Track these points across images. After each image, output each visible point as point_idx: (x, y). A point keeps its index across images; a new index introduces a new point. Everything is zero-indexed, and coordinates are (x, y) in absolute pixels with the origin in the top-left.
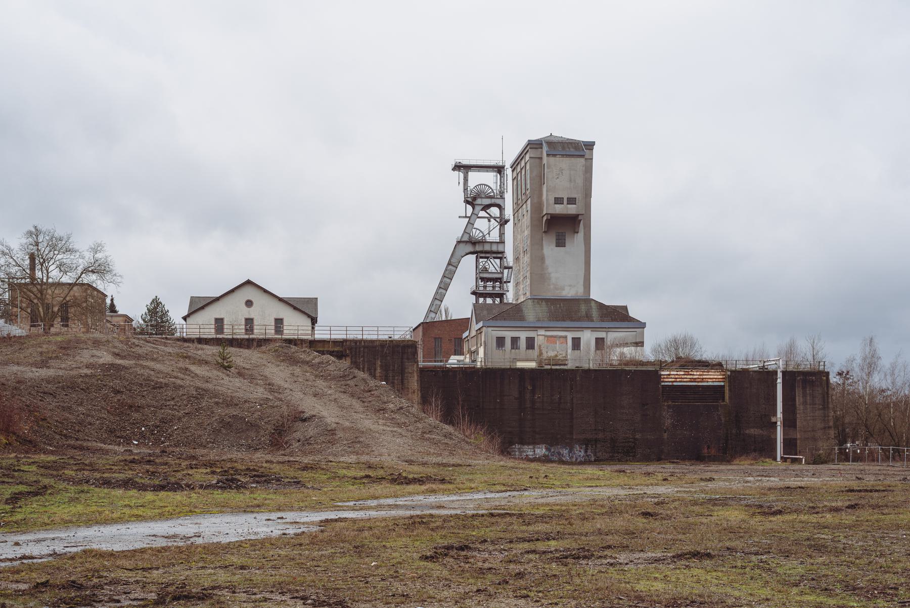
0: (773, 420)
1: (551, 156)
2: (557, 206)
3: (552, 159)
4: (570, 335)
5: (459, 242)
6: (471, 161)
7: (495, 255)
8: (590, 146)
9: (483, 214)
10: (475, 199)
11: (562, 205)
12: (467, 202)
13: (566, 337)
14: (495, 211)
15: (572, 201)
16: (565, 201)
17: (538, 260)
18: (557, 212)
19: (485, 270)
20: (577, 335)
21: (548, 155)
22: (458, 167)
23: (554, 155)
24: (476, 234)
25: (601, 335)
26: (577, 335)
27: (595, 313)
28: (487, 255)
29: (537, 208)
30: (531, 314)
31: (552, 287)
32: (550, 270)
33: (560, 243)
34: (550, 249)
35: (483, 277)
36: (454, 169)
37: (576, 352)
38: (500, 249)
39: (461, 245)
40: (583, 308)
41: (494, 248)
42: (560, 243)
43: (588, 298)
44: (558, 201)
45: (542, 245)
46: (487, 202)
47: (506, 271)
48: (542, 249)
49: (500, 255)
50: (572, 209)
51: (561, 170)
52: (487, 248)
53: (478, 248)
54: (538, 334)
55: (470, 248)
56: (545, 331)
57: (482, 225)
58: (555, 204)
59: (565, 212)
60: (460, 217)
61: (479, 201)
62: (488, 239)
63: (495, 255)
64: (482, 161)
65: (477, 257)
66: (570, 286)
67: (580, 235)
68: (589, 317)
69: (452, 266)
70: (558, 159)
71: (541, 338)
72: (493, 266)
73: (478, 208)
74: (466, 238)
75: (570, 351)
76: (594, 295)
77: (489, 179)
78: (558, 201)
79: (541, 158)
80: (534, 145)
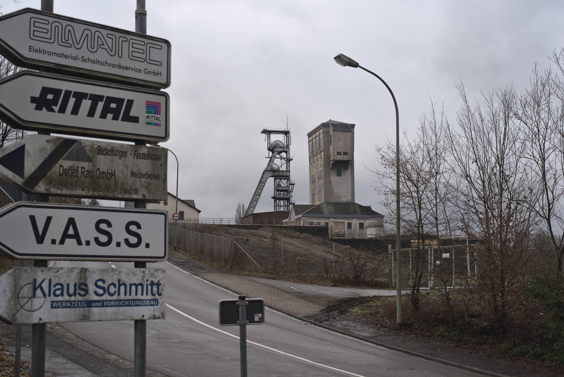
0: (465, 264)
2: (338, 156)
3: (335, 133)
4: (346, 222)
5: (266, 171)
7: (285, 178)
8: (353, 126)
9: (278, 156)
10: (274, 148)
12: (269, 149)
13: (344, 222)
14: (284, 155)
15: (345, 154)
16: (342, 154)
17: (328, 183)
18: (338, 159)
19: (280, 186)
20: (350, 221)
21: (333, 131)
22: (264, 132)
23: (336, 131)
24: (275, 167)
25: (362, 221)
26: (350, 221)
27: (358, 210)
28: (281, 178)
29: (327, 156)
30: (326, 210)
31: (335, 196)
32: (334, 188)
33: (339, 174)
34: (334, 178)
35: (278, 189)
36: (262, 133)
37: (350, 230)
38: (288, 174)
39: (267, 173)
40: (352, 208)
41: (285, 174)
44: (339, 153)
45: (330, 176)
46: (280, 150)
47: (291, 186)
48: (330, 177)
50: (345, 158)
51: (340, 138)
52: (281, 174)
53: (276, 174)
55: (272, 174)
57: (278, 162)
58: (337, 155)
59: (342, 159)
60: (266, 157)
61: (276, 149)
62: (281, 169)
63: (285, 178)
65: (275, 179)
66: (344, 196)
67: (349, 171)
68: (355, 212)
69: (262, 182)
70: (338, 133)
71: (332, 223)
72: (284, 183)
73: (276, 153)
75: (346, 229)
77: (281, 138)
78: (339, 153)
79: (328, 132)
80: (325, 125)
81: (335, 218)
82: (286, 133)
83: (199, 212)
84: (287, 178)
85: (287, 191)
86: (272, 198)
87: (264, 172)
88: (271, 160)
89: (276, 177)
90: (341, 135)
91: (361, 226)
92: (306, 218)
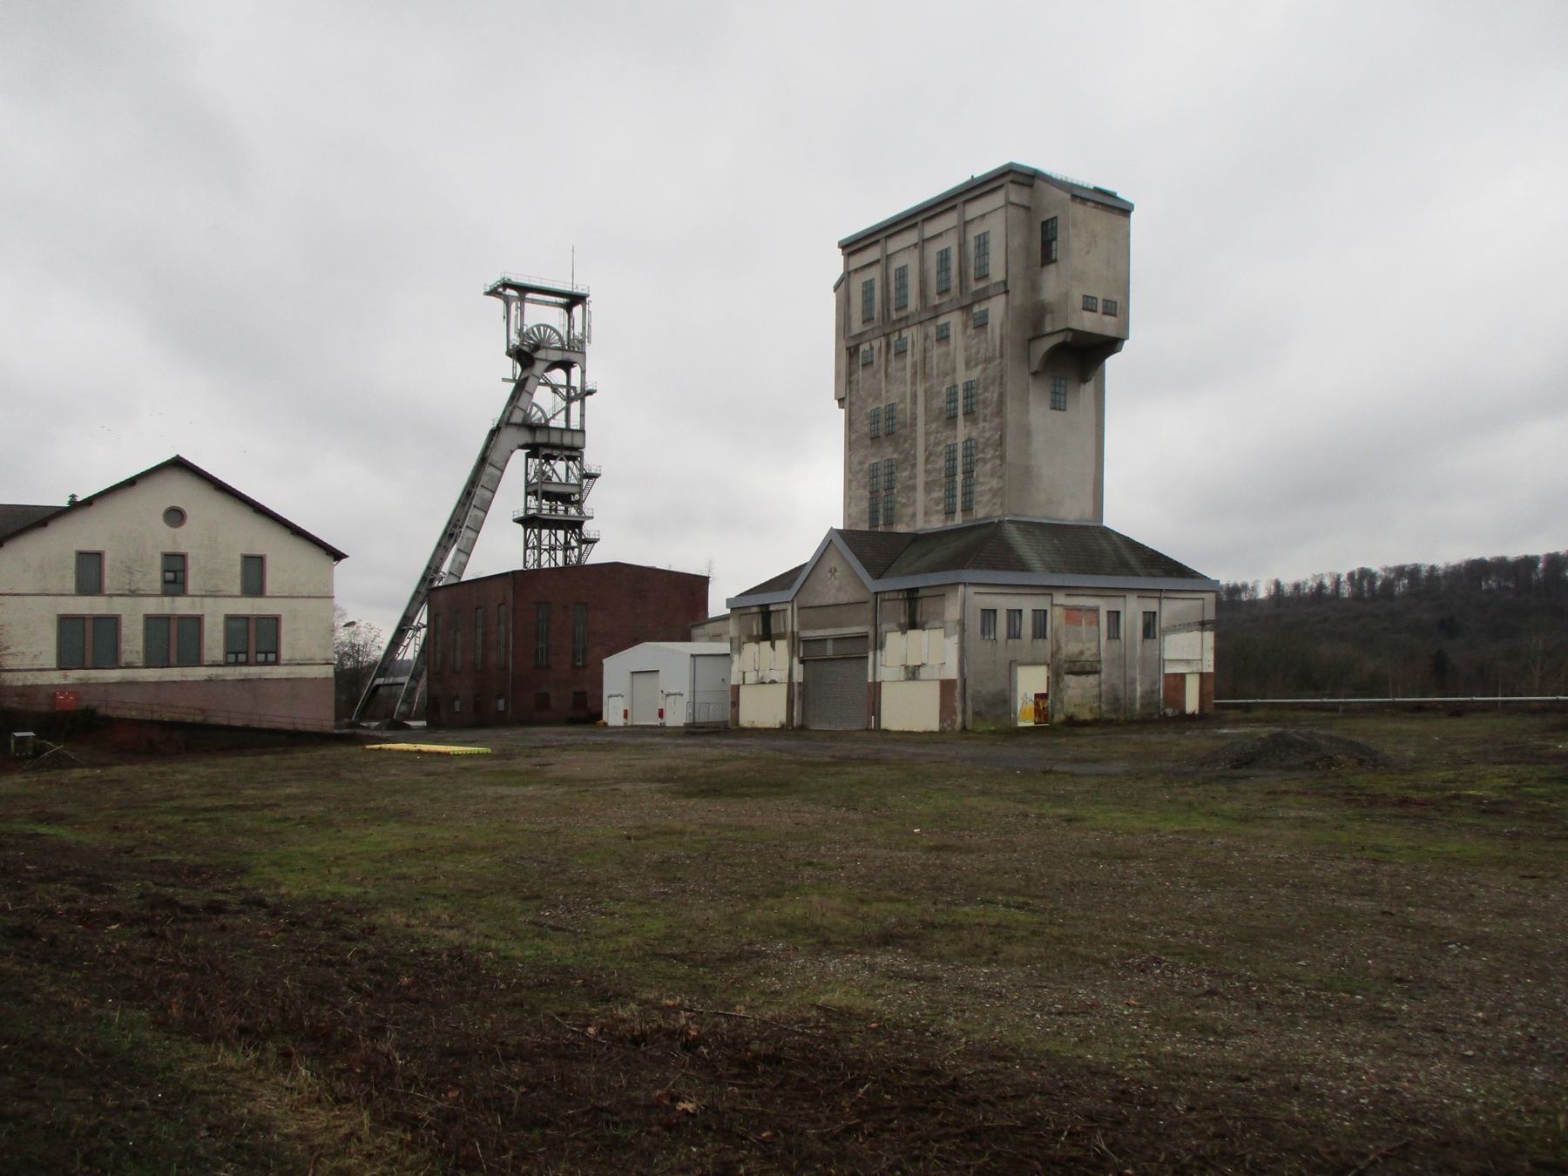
1: (1089, 204)
2: (1087, 314)
7: (567, 453)
11: (1094, 314)
22: (498, 290)
33: (1058, 405)
37: (1115, 643)
38: (577, 443)
41: (567, 440)
42: (1058, 405)
43: (1096, 524)
44: (1089, 304)
47: (585, 481)
49: (575, 454)
53: (540, 438)
55: (526, 437)
57: (544, 401)
59: (1097, 330)
60: (504, 380)
61: (541, 354)
62: (552, 424)
65: (528, 456)
67: (1089, 388)
74: (517, 417)
75: (1104, 639)
76: (1109, 521)
81: (1070, 590)
82: (573, 300)
83: (338, 556)
84: (573, 453)
86: (518, 521)
87: (494, 433)
88: (521, 386)
89: (534, 450)
90: (1099, 221)
91: (1150, 627)
92: (971, 590)
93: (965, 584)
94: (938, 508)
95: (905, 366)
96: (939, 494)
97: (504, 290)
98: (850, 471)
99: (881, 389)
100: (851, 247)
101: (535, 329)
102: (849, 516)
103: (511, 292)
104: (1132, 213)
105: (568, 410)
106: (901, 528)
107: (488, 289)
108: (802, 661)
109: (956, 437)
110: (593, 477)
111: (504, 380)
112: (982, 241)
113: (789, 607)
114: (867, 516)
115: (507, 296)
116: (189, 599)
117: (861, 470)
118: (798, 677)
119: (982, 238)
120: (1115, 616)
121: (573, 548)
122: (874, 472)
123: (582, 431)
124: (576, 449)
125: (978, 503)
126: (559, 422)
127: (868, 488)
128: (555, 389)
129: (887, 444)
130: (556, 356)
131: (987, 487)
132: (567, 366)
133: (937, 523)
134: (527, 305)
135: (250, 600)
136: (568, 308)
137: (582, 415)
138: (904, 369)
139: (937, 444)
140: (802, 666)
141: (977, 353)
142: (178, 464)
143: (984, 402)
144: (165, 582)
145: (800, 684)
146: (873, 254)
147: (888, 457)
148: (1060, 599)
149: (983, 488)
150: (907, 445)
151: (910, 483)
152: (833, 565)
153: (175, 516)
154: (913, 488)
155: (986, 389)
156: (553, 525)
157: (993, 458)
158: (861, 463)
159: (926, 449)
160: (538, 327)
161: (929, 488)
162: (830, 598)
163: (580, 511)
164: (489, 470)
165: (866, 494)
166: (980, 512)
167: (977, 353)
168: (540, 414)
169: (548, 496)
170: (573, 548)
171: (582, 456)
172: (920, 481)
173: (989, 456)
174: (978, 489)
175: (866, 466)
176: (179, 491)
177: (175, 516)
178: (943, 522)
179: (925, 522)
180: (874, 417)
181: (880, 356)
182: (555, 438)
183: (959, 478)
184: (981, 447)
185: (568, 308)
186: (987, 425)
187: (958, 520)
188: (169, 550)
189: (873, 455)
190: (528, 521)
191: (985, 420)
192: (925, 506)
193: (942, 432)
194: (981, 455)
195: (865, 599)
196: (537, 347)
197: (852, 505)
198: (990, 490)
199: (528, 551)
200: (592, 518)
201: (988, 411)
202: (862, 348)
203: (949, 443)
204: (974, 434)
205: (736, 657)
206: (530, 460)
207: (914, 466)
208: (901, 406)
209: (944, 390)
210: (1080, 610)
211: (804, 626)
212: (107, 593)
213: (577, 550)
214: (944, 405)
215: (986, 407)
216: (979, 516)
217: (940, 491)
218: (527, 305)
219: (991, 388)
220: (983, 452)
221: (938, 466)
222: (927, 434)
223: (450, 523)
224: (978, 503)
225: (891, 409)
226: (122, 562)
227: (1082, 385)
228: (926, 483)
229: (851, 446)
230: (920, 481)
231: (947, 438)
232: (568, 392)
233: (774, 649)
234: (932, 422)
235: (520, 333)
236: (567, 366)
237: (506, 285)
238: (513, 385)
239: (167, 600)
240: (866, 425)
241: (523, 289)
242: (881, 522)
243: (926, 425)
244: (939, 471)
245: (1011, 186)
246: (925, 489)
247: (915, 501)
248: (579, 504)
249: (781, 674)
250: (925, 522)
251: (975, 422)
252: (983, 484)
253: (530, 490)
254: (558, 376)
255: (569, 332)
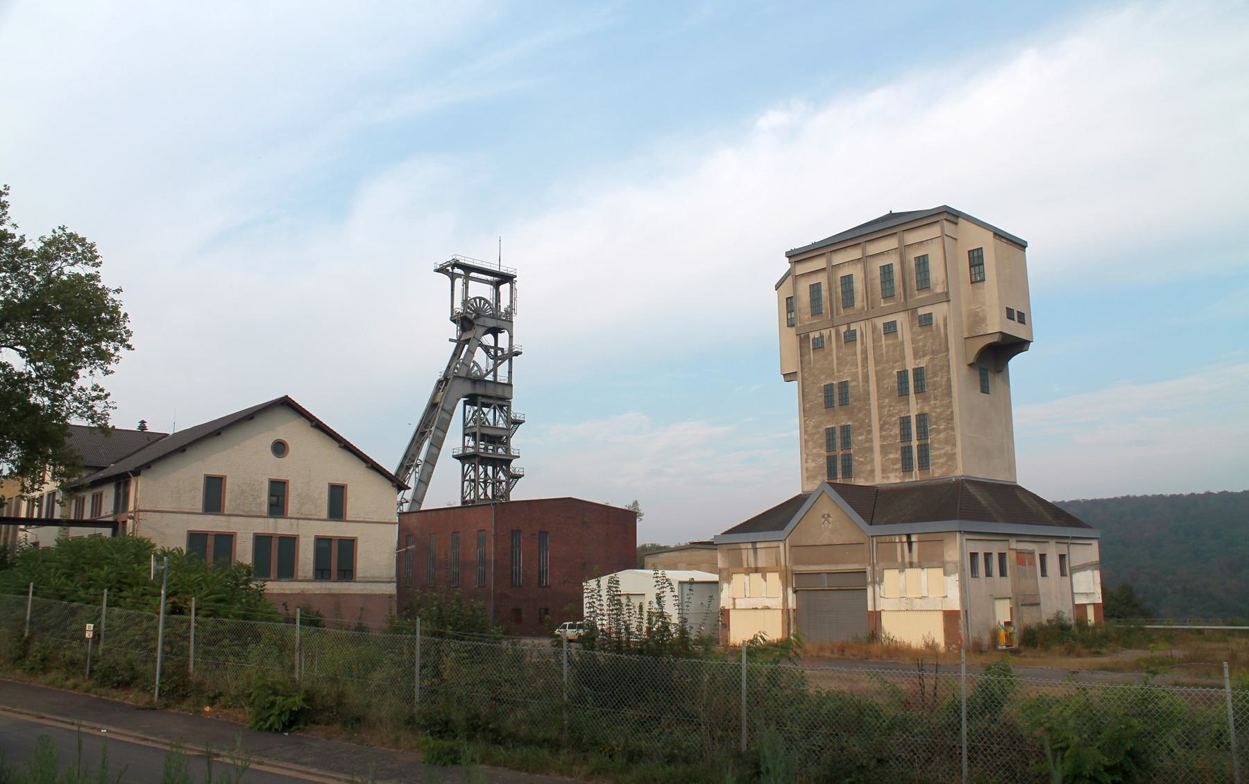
4: (1037, 549)
6: (484, 263)
28: (491, 401)
38: (507, 395)
41: (499, 392)
53: (479, 390)
54: (1011, 547)
55: (468, 389)
56: (1017, 541)
60: (451, 340)
61: (481, 321)
64: (489, 265)
65: (466, 403)
85: (498, 439)
86: (457, 457)
87: (443, 383)
89: (472, 400)
93: (960, 532)
94: (895, 467)
95: (856, 351)
96: (896, 455)
97: (453, 268)
98: (806, 432)
99: (833, 369)
100: (795, 256)
101: (478, 300)
102: (807, 469)
103: (457, 271)
104: (1027, 248)
105: (495, 370)
106: (861, 482)
107: (438, 267)
108: (795, 592)
109: (909, 411)
110: (518, 423)
111: (451, 340)
112: (921, 262)
113: (782, 545)
114: (825, 471)
115: (452, 273)
116: (289, 520)
117: (818, 433)
118: (792, 603)
119: (921, 259)
120: (1043, 557)
121: (501, 482)
122: (830, 433)
123: (510, 385)
124: (504, 399)
125: (934, 464)
126: (490, 378)
127: (825, 447)
128: (486, 349)
129: (842, 413)
130: (492, 323)
131: (942, 452)
132: (495, 331)
133: (895, 479)
134: (471, 283)
135: (333, 523)
136: (496, 285)
137: (510, 372)
138: (855, 354)
139: (891, 416)
140: (795, 595)
141: (925, 346)
142: (286, 404)
143: (934, 385)
144: (271, 505)
145: (794, 610)
146: (820, 263)
147: (843, 424)
148: (1014, 544)
149: (937, 453)
150: (861, 415)
151: (867, 445)
152: (825, 512)
153: (280, 448)
154: (871, 449)
155: (935, 375)
156: (485, 461)
157: (945, 429)
158: (816, 427)
159: (880, 419)
160: (475, 299)
161: (885, 450)
162: (825, 537)
163: (507, 450)
164: (439, 414)
165: (823, 452)
166: (937, 472)
167: (925, 346)
168: (476, 368)
169: (484, 437)
170: (501, 482)
171: (509, 407)
172: (877, 444)
173: (942, 427)
174: (932, 453)
175: (822, 430)
176: (288, 429)
177: (280, 448)
178: (900, 479)
179: (883, 477)
180: (828, 389)
181: (831, 342)
182: (490, 392)
183: (915, 443)
184: (934, 420)
185: (496, 285)
186: (938, 403)
187: (916, 476)
188: (275, 477)
189: (829, 421)
190: (463, 458)
191: (935, 399)
192: (882, 465)
193: (895, 406)
194: (935, 426)
195: (862, 542)
196: (478, 316)
197: (809, 461)
198: (946, 454)
199: (466, 483)
200: (519, 457)
201: (939, 392)
202: (812, 335)
203: (903, 415)
204: (926, 409)
205: (725, 586)
206: (468, 407)
207: (870, 432)
208: (852, 384)
209: (895, 372)
210: (1024, 553)
211: (797, 561)
212: (226, 512)
213: (504, 483)
214: (896, 385)
215: (935, 389)
216: (936, 475)
217: (897, 453)
218: (471, 283)
219: (940, 374)
220: (935, 423)
221: (892, 433)
222: (880, 407)
223: (405, 456)
224: (934, 464)
225: (844, 386)
226: (239, 486)
227: (997, 374)
228: (882, 447)
229: (806, 412)
230: (877, 444)
231: (900, 411)
232: (496, 353)
233: (766, 581)
234: (885, 398)
235: (465, 302)
236: (495, 331)
237: (457, 264)
238: (456, 344)
239: (272, 520)
240: (820, 397)
241: (468, 269)
242: (839, 476)
243: (878, 400)
244: (896, 436)
245: (945, 222)
246: (881, 452)
247: (872, 461)
248: (506, 445)
249: (777, 603)
250: (883, 477)
251: (926, 400)
252: (938, 449)
253: (467, 431)
254: (488, 339)
255: (496, 304)
